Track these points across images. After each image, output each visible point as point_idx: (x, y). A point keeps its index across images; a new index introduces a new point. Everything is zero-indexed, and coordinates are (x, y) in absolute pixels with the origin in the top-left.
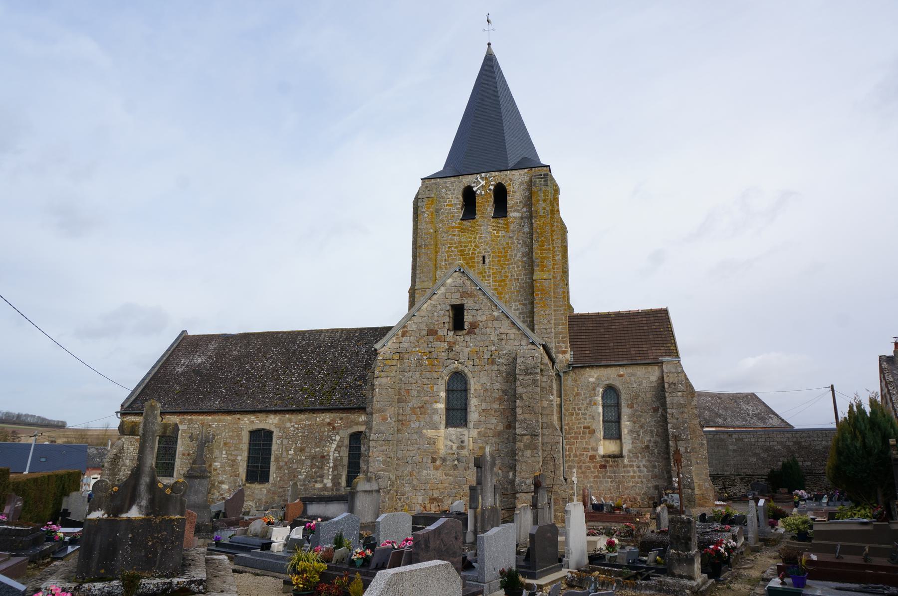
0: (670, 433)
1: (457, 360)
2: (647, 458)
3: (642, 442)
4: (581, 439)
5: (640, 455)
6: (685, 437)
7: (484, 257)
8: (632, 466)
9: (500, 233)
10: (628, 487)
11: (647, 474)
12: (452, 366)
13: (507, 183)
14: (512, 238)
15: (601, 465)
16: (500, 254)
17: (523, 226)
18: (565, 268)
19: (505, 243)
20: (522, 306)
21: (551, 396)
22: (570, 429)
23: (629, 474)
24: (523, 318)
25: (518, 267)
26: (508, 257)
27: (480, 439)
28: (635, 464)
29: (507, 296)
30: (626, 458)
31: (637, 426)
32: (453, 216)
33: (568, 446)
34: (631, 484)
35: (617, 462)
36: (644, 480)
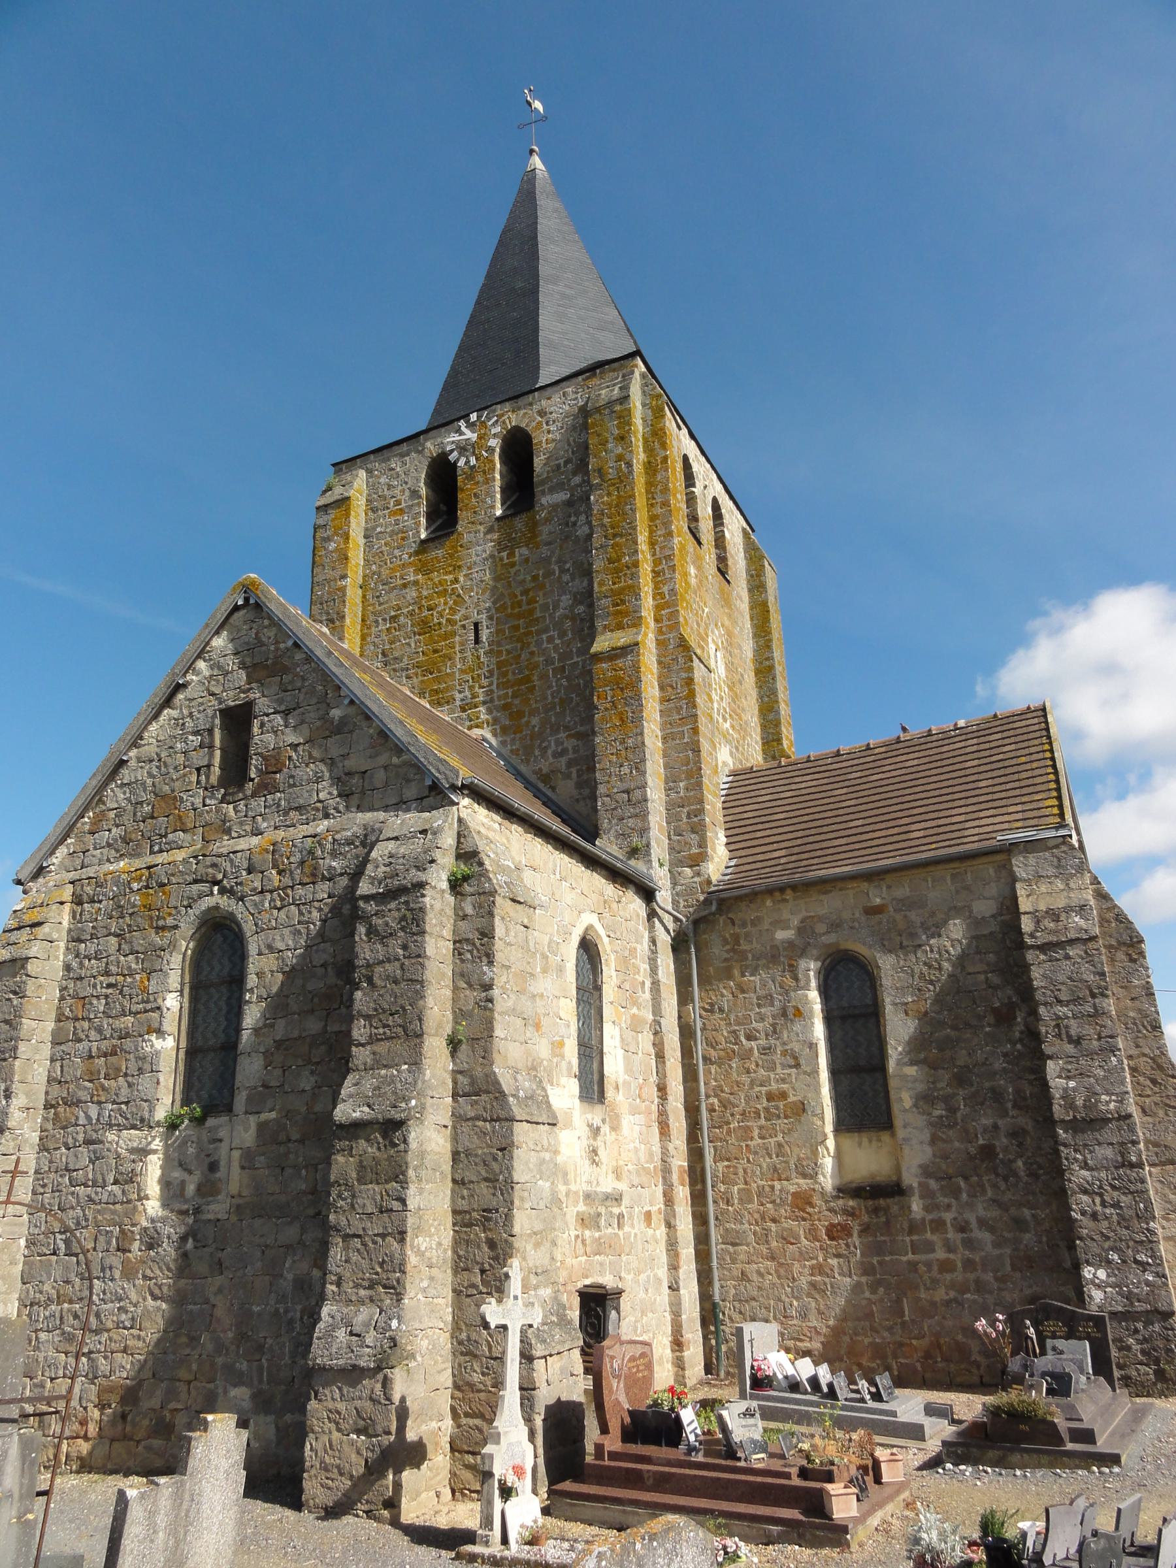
0: (1057, 1094)
1: (216, 883)
2: (990, 1193)
3: (968, 1136)
4: (762, 1137)
5: (962, 1184)
6: (1112, 1106)
7: (476, 625)
8: (938, 1225)
9: (517, 554)
10: (933, 1304)
11: (997, 1252)
12: (208, 902)
13: (534, 424)
14: (546, 561)
15: (832, 1225)
16: (516, 610)
17: (575, 524)
18: (767, 659)
19: (529, 578)
20: (573, 742)
21: (485, 968)
22: (724, 1105)
23: (931, 1256)
24: (578, 776)
25: (562, 634)
26: (538, 614)
27: (263, 1154)
28: (948, 1217)
29: (535, 721)
30: (917, 1195)
31: (945, 1076)
32: (403, 539)
33: (721, 1165)
34: (941, 1294)
35: (886, 1210)
36: (989, 1277)
